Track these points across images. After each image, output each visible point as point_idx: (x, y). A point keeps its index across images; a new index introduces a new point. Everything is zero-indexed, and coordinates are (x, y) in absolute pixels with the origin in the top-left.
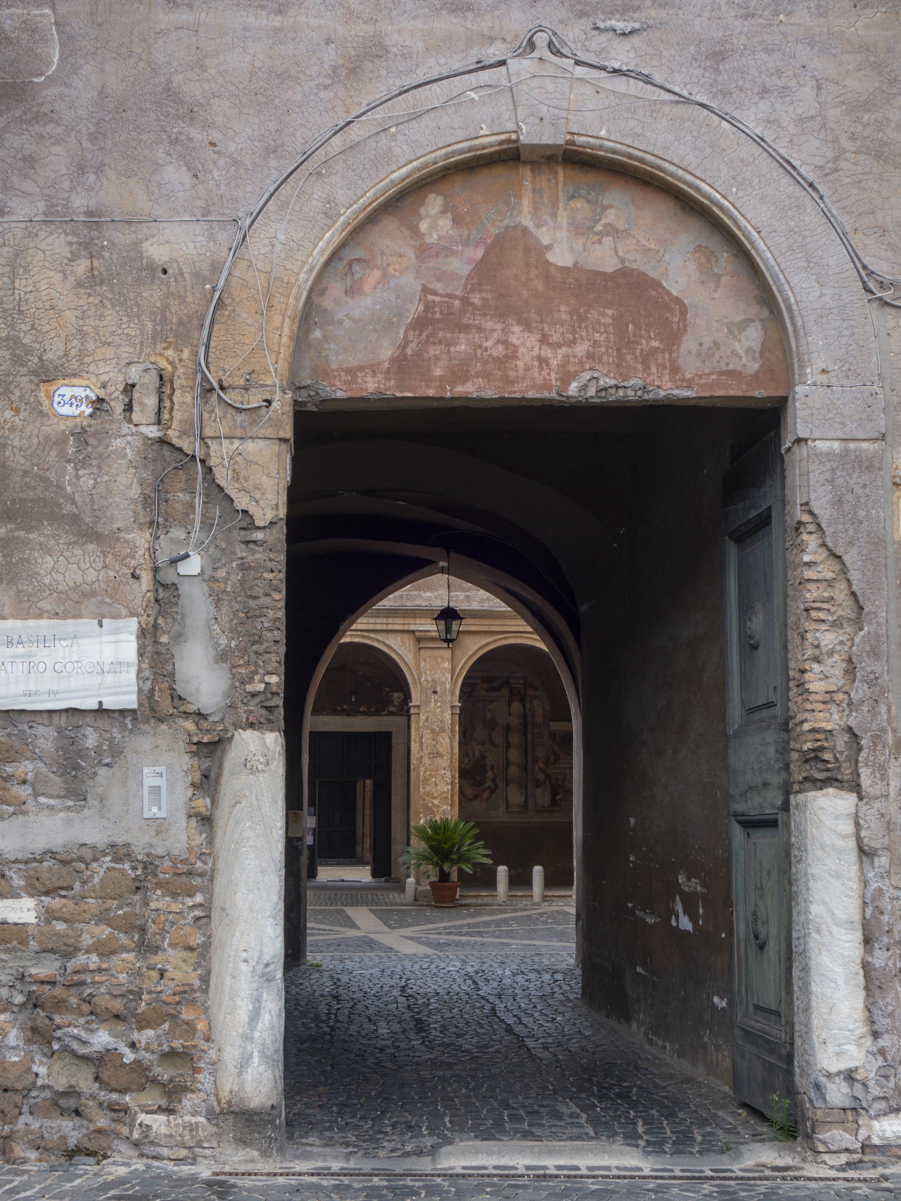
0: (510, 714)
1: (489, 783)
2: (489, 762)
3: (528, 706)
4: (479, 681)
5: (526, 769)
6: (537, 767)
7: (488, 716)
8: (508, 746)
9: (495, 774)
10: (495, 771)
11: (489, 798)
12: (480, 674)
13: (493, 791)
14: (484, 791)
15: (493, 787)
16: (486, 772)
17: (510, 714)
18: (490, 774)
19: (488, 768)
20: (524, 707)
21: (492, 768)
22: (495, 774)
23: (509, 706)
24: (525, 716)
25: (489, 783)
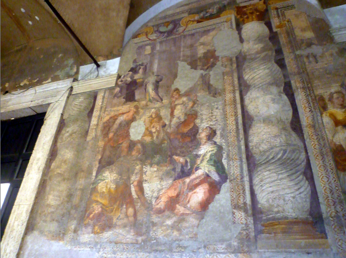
0: (242, 40)
1: (205, 168)
2: (203, 125)
3: (275, 22)
4: (186, 15)
5: (296, 125)
6: (326, 119)
7: (201, 51)
8: (243, 88)
9: (220, 148)
10: (218, 139)
11: (204, 205)
12: (186, 8)
13: (214, 189)
14: (193, 187)
15: (215, 177)
16: (198, 145)
17: (242, 40)
18: (206, 150)
19: (203, 135)
20: (269, 25)
21: (212, 134)
22: (220, 148)
23: (239, 27)
24: (273, 37)
25: (205, 168)
